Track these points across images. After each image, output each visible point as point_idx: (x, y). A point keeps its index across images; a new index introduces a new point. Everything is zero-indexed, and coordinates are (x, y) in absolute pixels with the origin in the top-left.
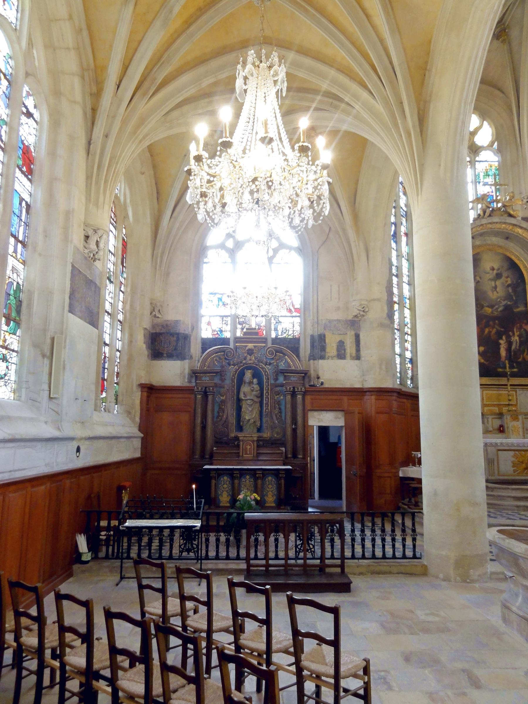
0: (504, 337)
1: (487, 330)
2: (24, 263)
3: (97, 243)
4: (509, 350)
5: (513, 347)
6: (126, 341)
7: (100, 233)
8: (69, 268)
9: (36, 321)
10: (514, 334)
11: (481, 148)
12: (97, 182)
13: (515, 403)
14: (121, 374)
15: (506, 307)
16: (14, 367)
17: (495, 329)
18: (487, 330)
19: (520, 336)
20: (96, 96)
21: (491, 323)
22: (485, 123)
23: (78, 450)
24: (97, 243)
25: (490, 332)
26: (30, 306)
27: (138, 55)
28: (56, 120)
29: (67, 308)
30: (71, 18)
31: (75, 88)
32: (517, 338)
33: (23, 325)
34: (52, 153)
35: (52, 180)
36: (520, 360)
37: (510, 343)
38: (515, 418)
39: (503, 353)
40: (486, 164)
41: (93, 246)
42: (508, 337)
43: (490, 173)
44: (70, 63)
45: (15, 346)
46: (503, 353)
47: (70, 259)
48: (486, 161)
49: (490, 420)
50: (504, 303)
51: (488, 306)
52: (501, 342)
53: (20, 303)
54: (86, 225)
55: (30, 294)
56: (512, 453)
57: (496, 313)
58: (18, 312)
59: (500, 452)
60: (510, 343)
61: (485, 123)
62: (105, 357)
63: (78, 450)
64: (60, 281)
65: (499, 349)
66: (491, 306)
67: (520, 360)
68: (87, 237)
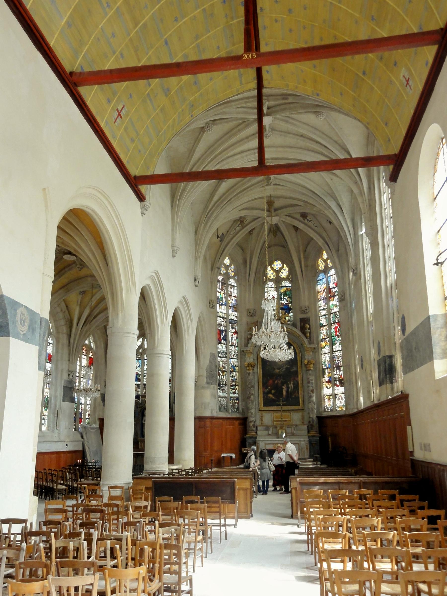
0: (285, 385)
1: (276, 382)
2: (49, 389)
3: (72, 376)
4: (287, 392)
5: (290, 390)
6: (93, 401)
7: (73, 373)
8: (63, 387)
9: (53, 406)
10: (290, 382)
11: (284, 279)
12: (72, 354)
13: (290, 419)
14: (91, 415)
15: (287, 368)
16: (46, 421)
17: (280, 381)
18: (276, 382)
19: (293, 384)
20: (71, 327)
21: (279, 378)
22: (285, 265)
23: (67, 445)
24: (72, 376)
25: (278, 383)
26: (51, 401)
27: (82, 316)
28: (58, 341)
29: (62, 400)
30: (62, 310)
31: (65, 329)
32: (292, 385)
33: (49, 408)
34: (57, 352)
35: (57, 361)
36: (293, 396)
37: (288, 388)
38: (282, 428)
39: (284, 393)
40: (285, 288)
41: (71, 377)
42: (287, 385)
43: (287, 293)
44: (62, 322)
45: (47, 415)
46: (284, 393)
47: (63, 385)
48: (285, 287)
49: (271, 429)
50: (285, 367)
51: (277, 369)
52: (284, 387)
53: (48, 401)
54: (68, 370)
55: (51, 398)
56: (272, 445)
57: (281, 373)
58: (48, 404)
59: (267, 445)
60: (288, 388)
61: (285, 265)
62: (82, 409)
63: (67, 445)
64: (60, 392)
65: (282, 391)
66: (279, 369)
67: (293, 396)
68: (69, 375)
